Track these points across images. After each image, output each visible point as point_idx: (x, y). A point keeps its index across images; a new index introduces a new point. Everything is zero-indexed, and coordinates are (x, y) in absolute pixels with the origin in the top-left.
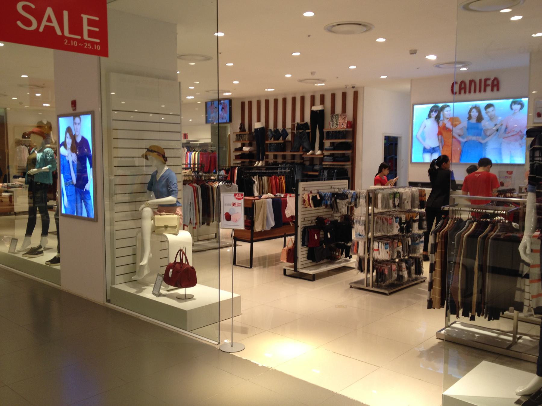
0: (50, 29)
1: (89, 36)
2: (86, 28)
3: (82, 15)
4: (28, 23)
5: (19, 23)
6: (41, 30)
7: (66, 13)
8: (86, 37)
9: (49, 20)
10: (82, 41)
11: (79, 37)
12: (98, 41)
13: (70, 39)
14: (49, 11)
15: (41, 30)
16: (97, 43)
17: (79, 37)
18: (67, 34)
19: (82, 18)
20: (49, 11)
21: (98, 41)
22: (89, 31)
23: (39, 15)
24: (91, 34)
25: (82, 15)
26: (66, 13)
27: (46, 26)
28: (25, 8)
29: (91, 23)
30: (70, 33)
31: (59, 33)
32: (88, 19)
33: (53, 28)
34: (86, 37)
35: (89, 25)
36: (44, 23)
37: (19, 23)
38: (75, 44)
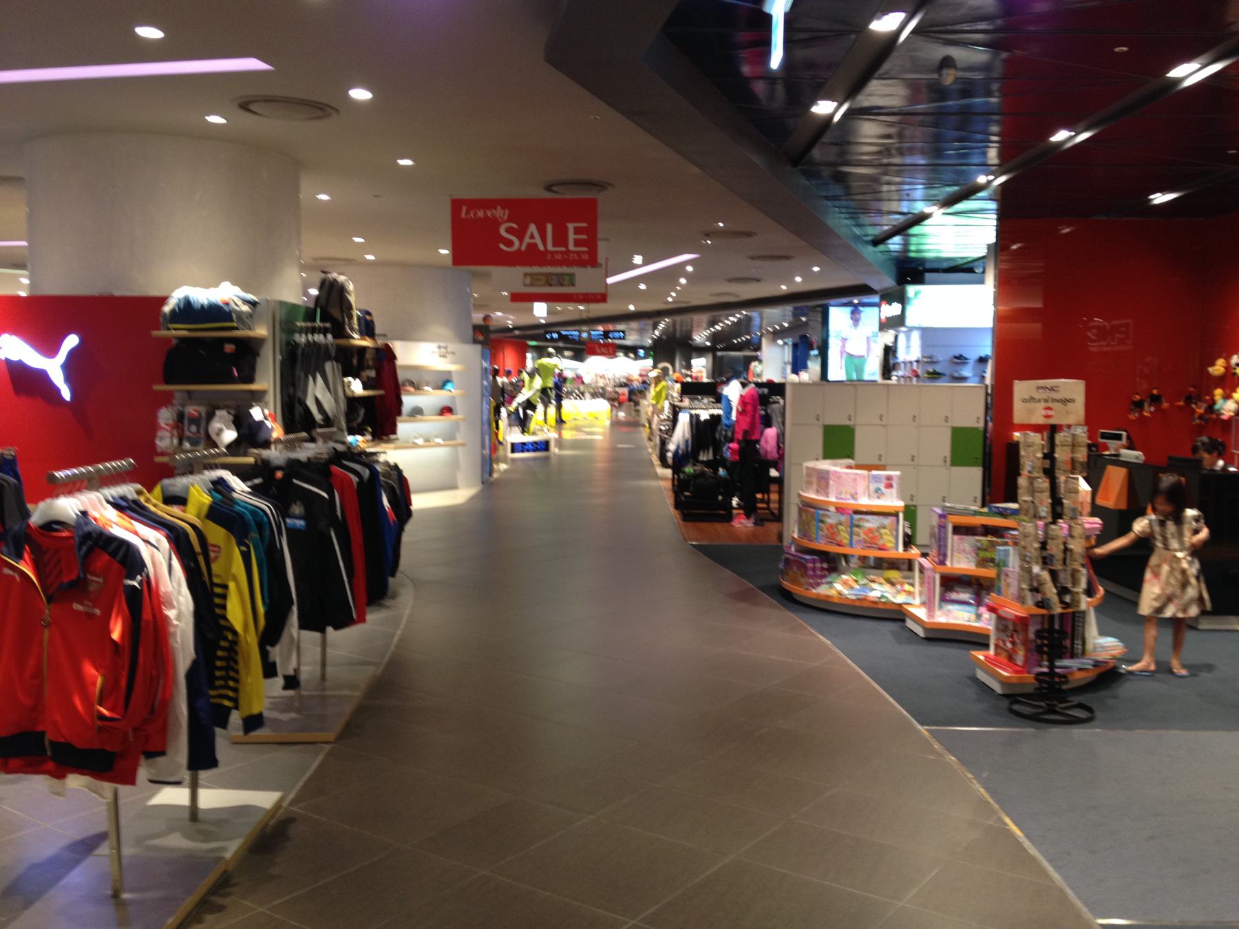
0: (532, 247)
2: (572, 236)
4: (510, 243)
5: (502, 246)
6: (523, 248)
7: (549, 227)
8: (572, 247)
9: (532, 237)
10: (568, 252)
11: (563, 249)
12: (585, 249)
13: (552, 253)
14: (532, 228)
17: (563, 249)
18: (550, 247)
20: (532, 228)
23: (520, 235)
24: (577, 243)
26: (549, 227)
27: (529, 245)
28: (508, 230)
29: (578, 231)
30: (554, 245)
31: (541, 247)
33: (535, 245)
34: (572, 247)
36: (527, 240)
37: (502, 246)
38: (559, 257)
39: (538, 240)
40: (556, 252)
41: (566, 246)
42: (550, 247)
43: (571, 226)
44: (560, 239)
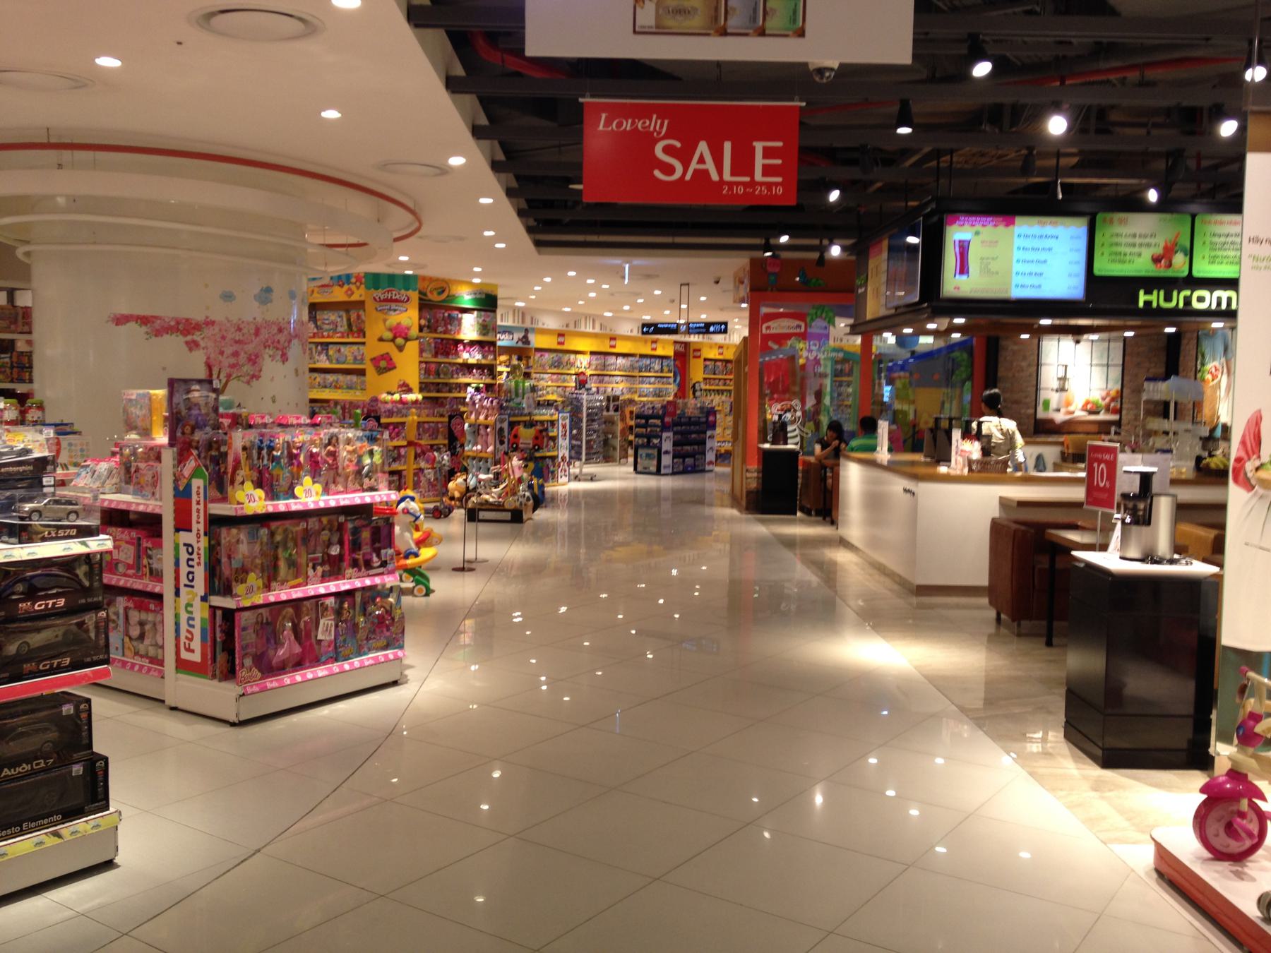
0: (702, 175)
1: (765, 174)
2: (759, 161)
3: (755, 144)
4: (669, 170)
5: (657, 173)
6: (688, 177)
7: (727, 146)
9: (702, 160)
10: (753, 183)
11: (747, 179)
12: (779, 179)
13: (731, 184)
14: (703, 147)
15: (688, 177)
16: (777, 184)
17: (747, 179)
18: (727, 176)
19: (754, 148)
20: (703, 147)
21: (779, 179)
22: (764, 166)
23: (685, 156)
24: (767, 170)
25: (755, 144)
26: (727, 146)
27: (696, 172)
28: (668, 150)
29: (768, 153)
30: (733, 174)
31: (715, 176)
32: (765, 149)
33: (706, 172)
34: (758, 176)
35: (765, 156)
36: (694, 165)
37: (657, 173)
39: (710, 165)
40: (738, 184)
41: (752, 174)
42: (727, 176)
43: (759, 146)
44: (743, 163)
